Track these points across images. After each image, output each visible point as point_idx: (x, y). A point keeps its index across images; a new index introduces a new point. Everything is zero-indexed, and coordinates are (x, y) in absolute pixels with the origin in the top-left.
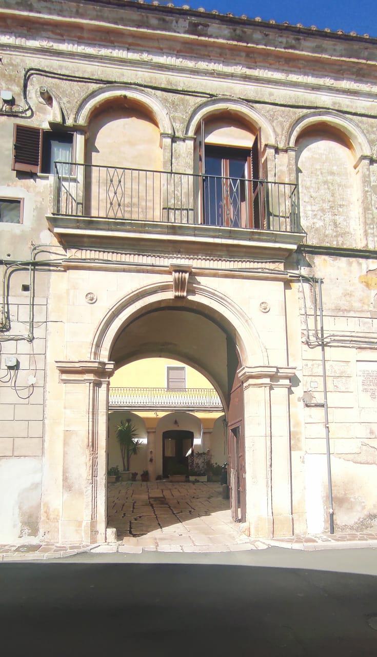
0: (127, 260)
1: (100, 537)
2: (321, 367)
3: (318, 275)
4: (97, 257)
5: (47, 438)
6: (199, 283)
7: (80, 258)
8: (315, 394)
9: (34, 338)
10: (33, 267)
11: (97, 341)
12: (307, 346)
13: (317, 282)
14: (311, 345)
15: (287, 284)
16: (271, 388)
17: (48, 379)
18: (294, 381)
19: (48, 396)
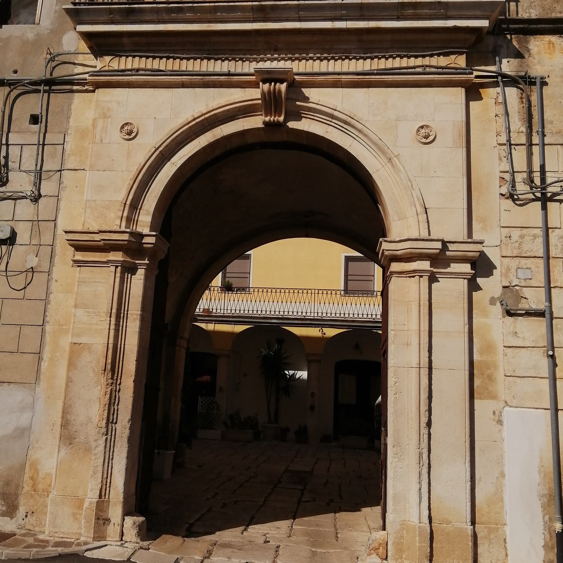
0: (190, 68)
1: (112, 530)
2: (540, 241)
3: (536, 71)
4: (142, 66)
5: (46, 355)
6: (306, 99)
7: (116, 68)
8: (526, 292)
9: (40, 196)
10: (47, 88)
11: (132, 200)
12: (510, 202)
13: (534, 84)
14: (518, 199)
15: (473, 92)
16: (433, 279)
17: (57, 259)
18: (481, 266)
19: (54, 286)
